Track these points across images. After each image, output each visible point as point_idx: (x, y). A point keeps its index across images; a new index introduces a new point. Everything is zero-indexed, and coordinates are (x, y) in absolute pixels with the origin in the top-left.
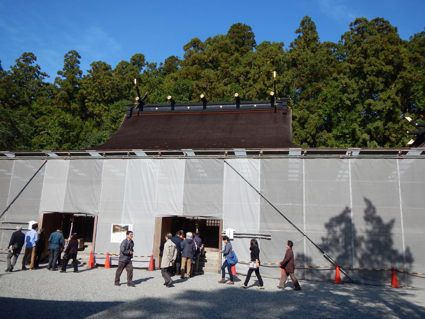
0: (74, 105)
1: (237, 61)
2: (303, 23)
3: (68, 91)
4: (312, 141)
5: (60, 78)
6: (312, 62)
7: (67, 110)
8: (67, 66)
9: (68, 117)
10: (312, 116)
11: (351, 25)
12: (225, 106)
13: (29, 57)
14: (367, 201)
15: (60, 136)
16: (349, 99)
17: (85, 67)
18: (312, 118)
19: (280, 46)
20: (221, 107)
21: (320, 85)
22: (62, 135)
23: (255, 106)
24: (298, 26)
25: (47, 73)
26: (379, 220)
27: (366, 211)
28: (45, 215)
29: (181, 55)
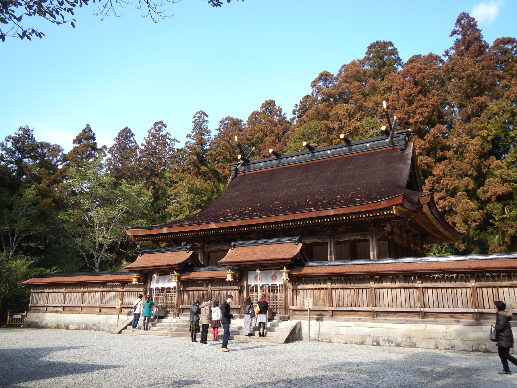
0: (204, 169)
1: (374, 88)
3: (198, 154)
4: (475, 174)
5: (190, 142)
6: (469, 72)
7: (198, 174)
8: (195, 127)
9: (198, 183)
10: (472, 141)
12: (333, 150)
13: (160, 125)
15: (191, 202)
17: (213, 127)
18: (472, 144)
19: (432, 58)
20: (329, 152)
21: (482, 99)
22: (192, 201)
23: (368, 145)
24: (452, 26)
25: (177, 139)
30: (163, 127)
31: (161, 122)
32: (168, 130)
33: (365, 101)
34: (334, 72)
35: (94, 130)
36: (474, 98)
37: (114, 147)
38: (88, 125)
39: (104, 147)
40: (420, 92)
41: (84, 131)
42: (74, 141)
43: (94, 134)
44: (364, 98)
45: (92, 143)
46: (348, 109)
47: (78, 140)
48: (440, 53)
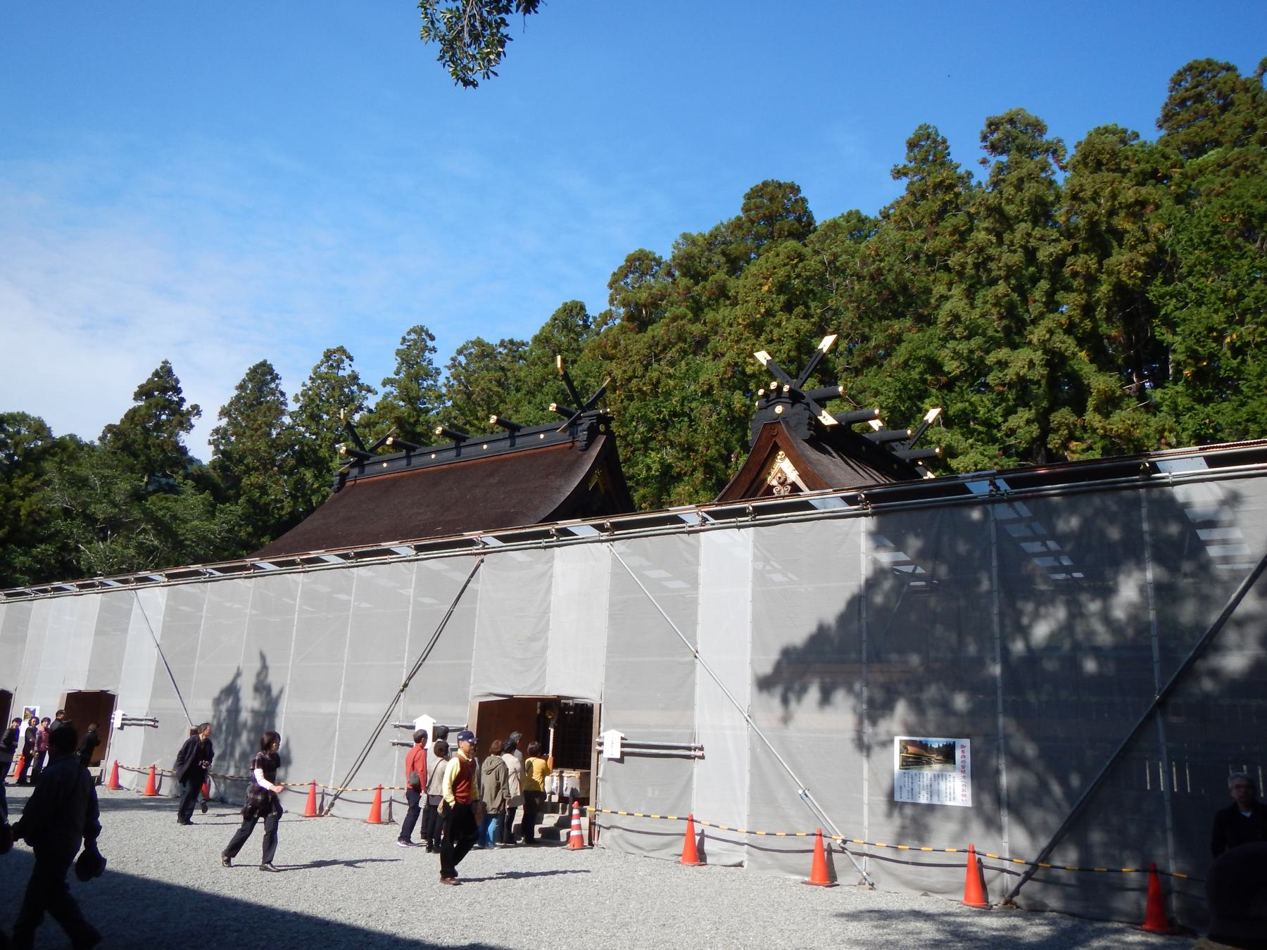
2: (912, 145)
11: (984, 138)
14: (263, 658)
16: (956, 355)
21: (897, 326)
24: (901, 158)
26: (268, 689)
27: (259, 675)
28: (482, 706)
29: (597, 303)
30: (347, 361)
31: (341, 350)
32: (357, 367)
33: (692, 322)
34: (665, 251)
35: (177, 372)
36: (885, 323)
37: (231, 404)
38: (166, 362)
39: (196, 410)
40: (788, 308)
41: (156, 374)
42: (137, 396)
43: (177, 381)
44: (690, 315)
45: (171, 402)
46: (653, 337)
47: (144, 392)
48: (871, 211)
